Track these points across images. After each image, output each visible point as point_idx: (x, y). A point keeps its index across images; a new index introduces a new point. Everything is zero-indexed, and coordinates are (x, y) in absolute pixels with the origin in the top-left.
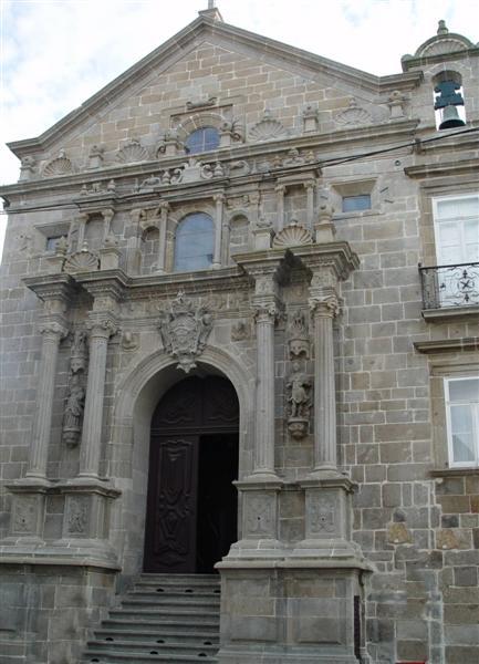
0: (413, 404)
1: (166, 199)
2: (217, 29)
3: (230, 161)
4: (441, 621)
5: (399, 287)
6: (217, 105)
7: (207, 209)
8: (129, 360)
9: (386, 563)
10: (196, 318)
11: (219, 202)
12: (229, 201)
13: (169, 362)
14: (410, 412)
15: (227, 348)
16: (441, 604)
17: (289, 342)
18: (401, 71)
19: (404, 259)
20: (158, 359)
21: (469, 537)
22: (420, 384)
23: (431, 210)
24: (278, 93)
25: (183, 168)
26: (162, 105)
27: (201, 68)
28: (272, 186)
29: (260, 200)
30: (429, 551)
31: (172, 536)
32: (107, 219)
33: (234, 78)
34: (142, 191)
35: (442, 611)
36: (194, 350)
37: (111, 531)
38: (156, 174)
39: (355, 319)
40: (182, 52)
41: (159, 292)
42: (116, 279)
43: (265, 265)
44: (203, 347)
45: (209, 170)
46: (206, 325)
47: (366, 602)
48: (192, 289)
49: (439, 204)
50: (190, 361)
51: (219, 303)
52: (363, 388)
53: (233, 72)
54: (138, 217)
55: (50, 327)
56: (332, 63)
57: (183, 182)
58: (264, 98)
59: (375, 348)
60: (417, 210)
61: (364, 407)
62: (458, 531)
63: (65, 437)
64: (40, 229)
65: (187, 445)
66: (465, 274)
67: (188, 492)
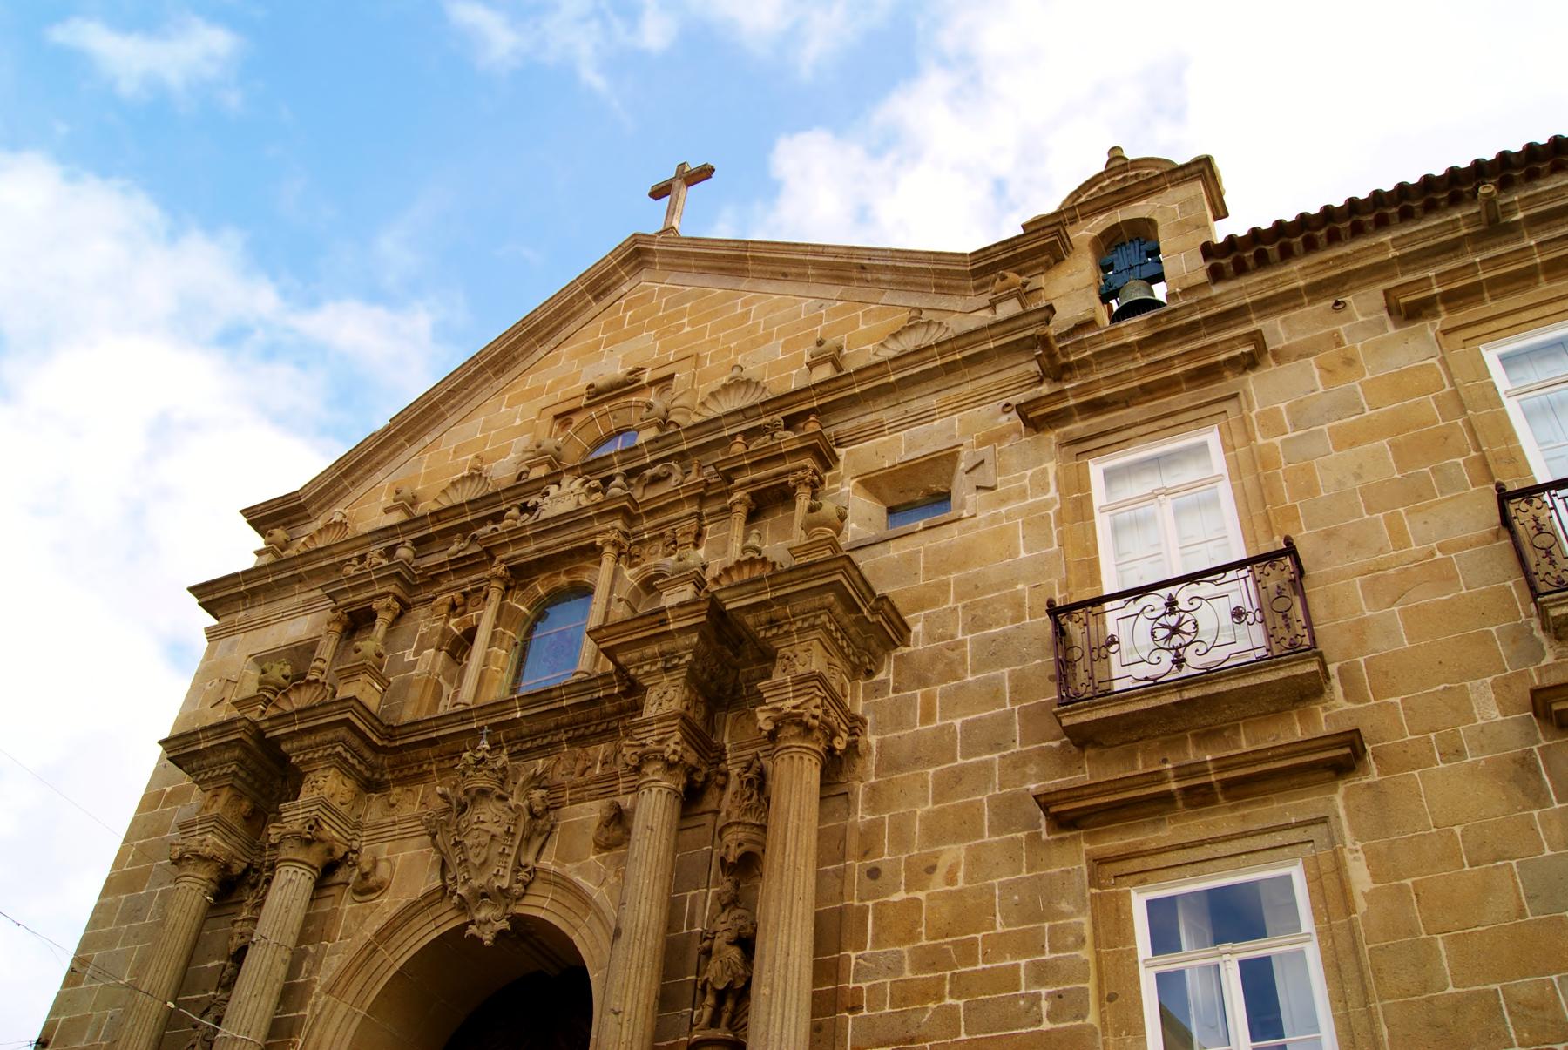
0: (1041, 973)
5: (1006, 671)
6: (645, 382)
10: (512, 802)
11: (608, 549)
13: (449, 921)
14: (1037, 997)
19: (1021, 605)
22: (1062, 915)
24: (768, 337)
26: (544, 400)
27: (626, 326)
33: (687, 329)
36: (505, 884)
39: (890, 763)
40: (596, 307)
42: (347, 722)
43: (666, 646)
44: (530, 878)
45: (596, 490)
48: (522, 738)
49: (1111, 476)
50: (499, 913)
51: (580, 766)
52: (902, 942)
53: (686, 320)
54: (445, 608)
58: (738, 352)
59: (936, 832)
60: (1053, 493)
61: (906, 995)
66: (1171, 604)
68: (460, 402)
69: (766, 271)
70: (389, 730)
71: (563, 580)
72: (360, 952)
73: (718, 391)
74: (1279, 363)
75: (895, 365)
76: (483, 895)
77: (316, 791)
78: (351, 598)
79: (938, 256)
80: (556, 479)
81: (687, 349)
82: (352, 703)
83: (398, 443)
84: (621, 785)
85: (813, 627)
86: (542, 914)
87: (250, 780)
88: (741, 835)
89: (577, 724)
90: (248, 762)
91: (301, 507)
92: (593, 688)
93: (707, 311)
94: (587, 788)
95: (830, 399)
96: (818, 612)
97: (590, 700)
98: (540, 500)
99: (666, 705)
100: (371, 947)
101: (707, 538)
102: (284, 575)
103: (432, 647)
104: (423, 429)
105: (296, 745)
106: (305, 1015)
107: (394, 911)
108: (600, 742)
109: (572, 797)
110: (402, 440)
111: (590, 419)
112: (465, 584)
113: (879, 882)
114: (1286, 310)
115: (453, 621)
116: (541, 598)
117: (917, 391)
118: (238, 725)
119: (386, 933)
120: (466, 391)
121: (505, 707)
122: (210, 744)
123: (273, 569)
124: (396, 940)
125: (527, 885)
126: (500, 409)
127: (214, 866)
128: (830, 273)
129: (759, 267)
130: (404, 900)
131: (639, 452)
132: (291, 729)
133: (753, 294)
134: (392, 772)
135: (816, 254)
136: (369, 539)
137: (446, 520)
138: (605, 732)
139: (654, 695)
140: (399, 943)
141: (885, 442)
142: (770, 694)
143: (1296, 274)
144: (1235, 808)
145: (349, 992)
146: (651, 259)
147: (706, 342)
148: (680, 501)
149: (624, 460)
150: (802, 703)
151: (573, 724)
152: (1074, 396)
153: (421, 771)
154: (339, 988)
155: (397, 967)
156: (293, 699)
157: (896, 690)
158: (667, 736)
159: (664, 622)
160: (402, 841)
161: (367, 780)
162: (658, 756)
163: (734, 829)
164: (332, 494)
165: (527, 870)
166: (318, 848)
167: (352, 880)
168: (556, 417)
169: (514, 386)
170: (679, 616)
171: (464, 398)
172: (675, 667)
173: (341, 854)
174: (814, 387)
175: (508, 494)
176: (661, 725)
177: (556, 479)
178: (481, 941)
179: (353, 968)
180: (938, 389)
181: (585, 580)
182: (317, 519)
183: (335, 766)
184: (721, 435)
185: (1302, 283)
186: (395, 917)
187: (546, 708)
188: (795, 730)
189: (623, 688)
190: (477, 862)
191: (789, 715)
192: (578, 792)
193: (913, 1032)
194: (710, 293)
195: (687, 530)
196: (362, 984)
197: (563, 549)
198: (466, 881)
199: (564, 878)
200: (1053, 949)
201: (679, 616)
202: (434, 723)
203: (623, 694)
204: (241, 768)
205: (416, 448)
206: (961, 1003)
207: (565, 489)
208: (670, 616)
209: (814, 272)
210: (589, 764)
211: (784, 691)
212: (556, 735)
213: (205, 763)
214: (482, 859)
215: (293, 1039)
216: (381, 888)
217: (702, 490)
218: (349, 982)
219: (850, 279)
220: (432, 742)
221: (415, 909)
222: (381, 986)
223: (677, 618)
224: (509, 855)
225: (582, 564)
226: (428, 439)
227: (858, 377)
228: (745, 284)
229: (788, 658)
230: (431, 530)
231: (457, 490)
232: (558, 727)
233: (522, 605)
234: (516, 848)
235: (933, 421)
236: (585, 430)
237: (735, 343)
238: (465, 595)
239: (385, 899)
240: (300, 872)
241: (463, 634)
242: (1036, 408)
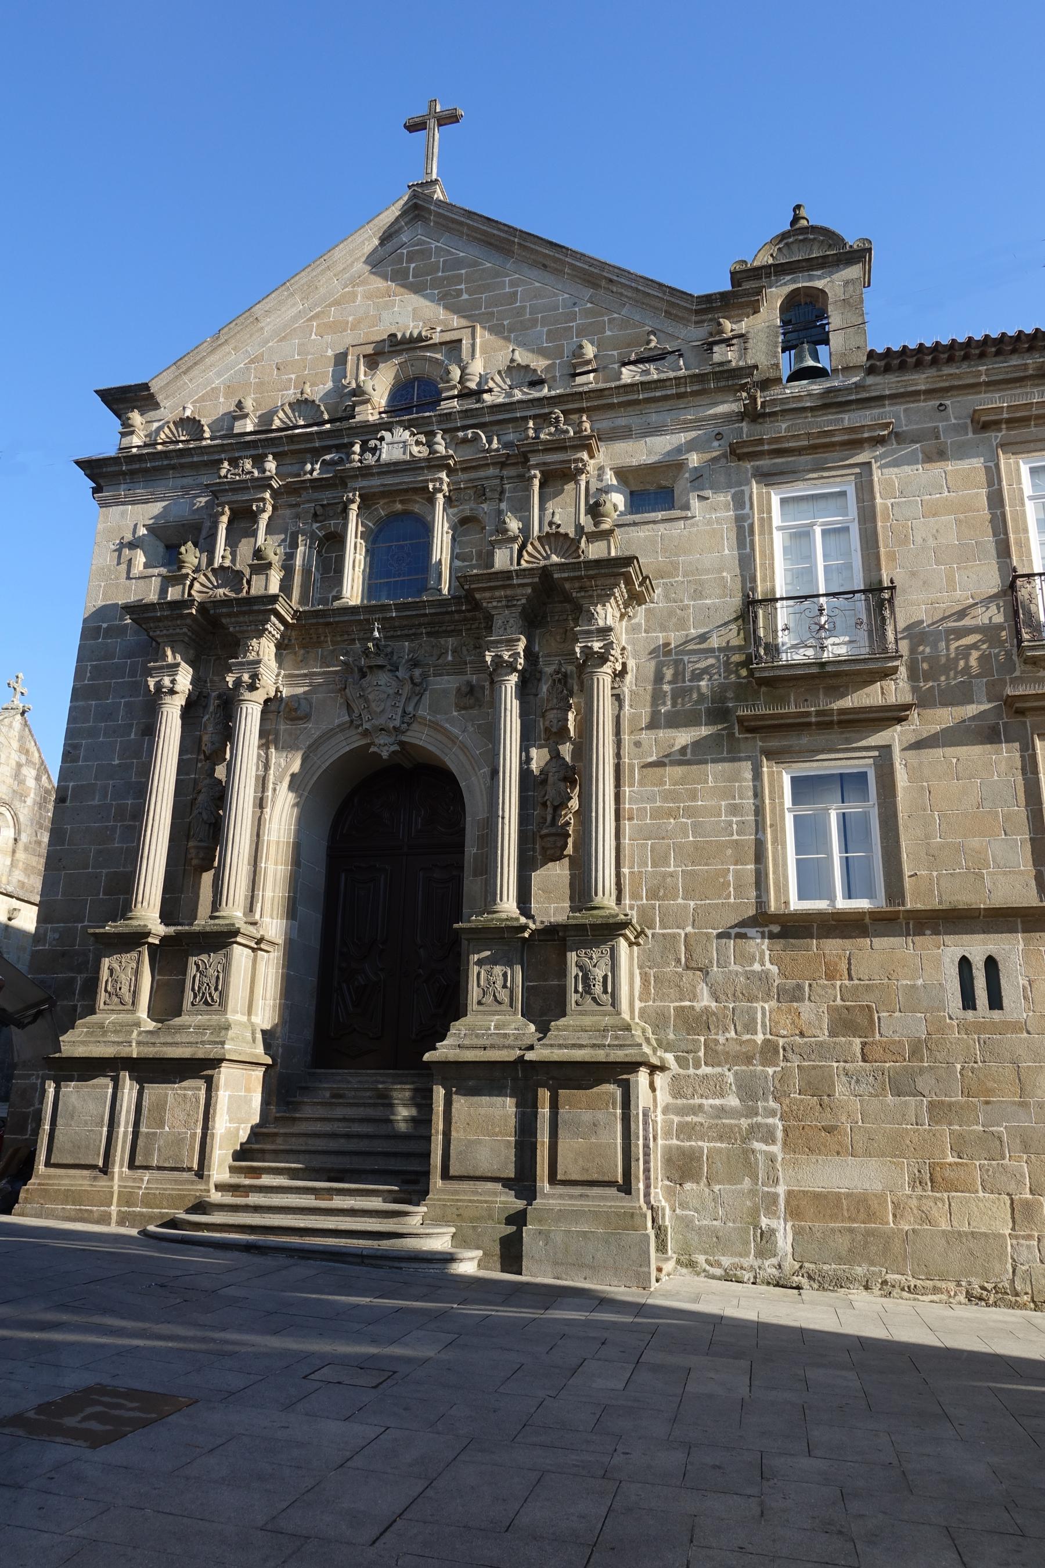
2: (439, 215)
3: (458, 429)
4: (776, 1149)
9: (690, 1056)
10: (399, 674)
16: (775, 1121)
17: (543, 716)
18: (728, 287)
20: (340, 737)
21: (820, 1019)
23: (769, 512)
24: (534, 322)
25: (382, 439)
27: (411, 279)
28: (521, 470)
29: (502, 492)
30: (759, 1038)
35: (779, 1134)
36: (397, 723)
38: (338, 448)
43: (509, 592)
44: (409, 719)
47: (660, 1118)
48: (394, 629)
50: (391, 740)
53: (463, 286)
62: (806, 1009)
71: (399, 507)
74: (899, 444)
80: (388, 426)
98: (378, 443)
105: (233, 620)
113: (641, 750)
114: (909, 402)
115: (315, 525)
125: (409, 724)
137: (299, 443)
138: (452, 631)
143: (920, 380)
144: (842, 733)
146: (427, 216)
147: (483, 314)
148: (488, 465)
152: (769, 444)
155: (324, 767)
157: (645, 632)
172: (514, 605)
175: (348, 432)
177: (388, 426)
178: (381, 756)
185: (923, 388)
186: (320, 737)
189: (469, 607)
190: (378, 710)
193: (664, 834)
200: (741, 798)
203: (468, 611)
206: (689, 821)
213: (161, 624)
232: (420, 625)
238: (322, 505)
242: (742, 447)
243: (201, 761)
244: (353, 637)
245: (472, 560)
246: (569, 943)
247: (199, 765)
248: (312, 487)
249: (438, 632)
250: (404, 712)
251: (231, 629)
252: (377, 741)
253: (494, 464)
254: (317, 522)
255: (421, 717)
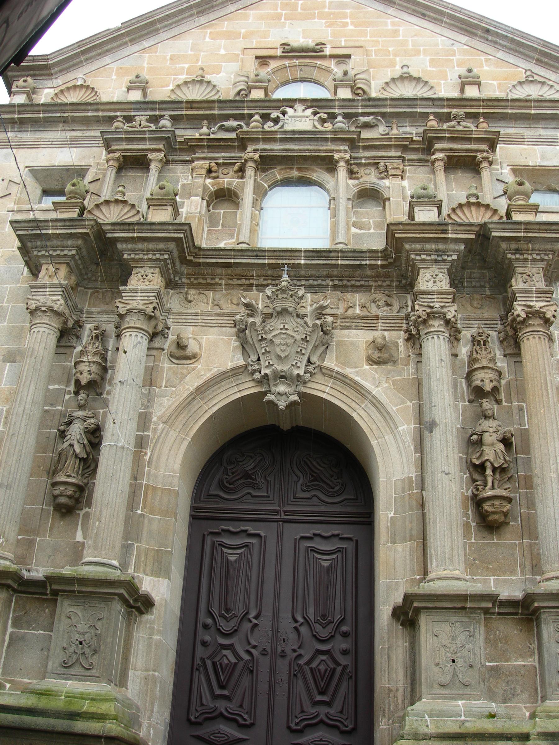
1: (256, 151)
7: (318, 175)
8: (183, 377)
11: (342, 164)
12: (355, 169)
15: (357, 373)
24: (418, 53)
25: (284, 113)
27: (299, 10)
31: (226, 692)
32: (153, 167)
34: (212, 136)
37: (131, 673)
38: (236, 117)
41: (240, 277)
43: (441, 246)
46: (325, 333)
51: (342, 306)
53: (348, 20)
54: (204, 172)
55: (49, 304)
56: (498, 24)
57: (288, 128)
58: (396, 55)
63: (56, 492)
64: (35, 172)
65: (258, 535)
67: (256, 617)
68: (171, 24)
69: (409, 8)
70: (197, 250)
71: (295, 173)
72: (185, 399)
73: (397, 79)
75: (536, 104)
76: (283, 377)
77: (147, 283)
78: (124, 146)
79: (546, 44)
81: (355, 41)
82: (186, 227)
83: (124, 40)
84: (380, 324)
85: (542, 260)
86: (324, 396)
87: (79, 262)
88: (491, 375)
89: (343, 277)
90: (84, 250)
91: (47, 67)
92: (362, 257)
93: (364, 20)
94: (354, 321)
95: (492, 111)
96: (548, 252)
97: (359, 265)
98: (281, 115)
99: (439, 284)
100: (192, 396)
101: (408, 175)
102: (54, 115)
103: (197, 196)
104: (142, 36)
105: (130, 246)
106: (148, 436)
107: (209, 375)
108: (356, 292)
109: (341, 324)
110: (127, 39)
111: (284, 66)
112: (219, 157)
115: (208, 181)
116: (277, 182)
117: (542, 124)
118: (87, 223)
119: (203, 389)
120: (177, 19)
121: (293, 254)
122: (58, 232)
123: (45, 108)
124: (209, 394)
125: (312, 374)
126: (204, 39)
127: (62, 319)
128: (461, 26)
129: (405, 4)
130: (216, 370)
131: (355, 104)
132: (131, 235)
133: (397, 20)
134: (189, 279)
135: (455, 11)
136: (132, 106)
138: (361, 286)
139: (428, 275)
140: (211, 397)
141: (525, 149)
142: (521, 295)
145: (177, 423)
149: (343, 106)
150: (544, 306)
151: (341, 277)
153: (213, 282)
154: (171, 421)
155: (210, 413)
156: (104, 210)
158: (447, 304)
159: (445, 231)
160: (204, 328)
161: (170, 280)
162: (442, 316)
163: (486, 371)
164: (71, 63)
165: (314, 366)
166: (153, 323)
167: (166, 346)
168: (257, 57)
169: (213, 25)
170: (457, 230)
171: (175, 22)
172: (444, 261)
173: (160, 329)
174: (483, 100)
176: (439, 296)
177: (290, 104)
179: (180, 409)
180: (556, 127)
181: (314, 178)
182: (56, 78)
183: (159, 268)
184: (415, 110)
186: (211, 380)
187: (325, 262)
188: (538, 321)
189: (384, 263)
191: (537, 312)
192: (348, 322)
194: (364, 8)
195: (395, 166)
196: (185, 420)
197: (304, 154)
198: (270, 365)
199: (345, 377)
201: (457, 230)
202: (233, 253)
203: (382, 266)
204: (78, 254)
205: (136, 47)
207: (299, 113)
208: (450, 228)
209: (448, 21)
210: (351, 305)
211: (530, 295)
212: (325, 280)
214: (287, 354)
215: (144, 450)
216: (195, 358)
217: (408, 143)
218: (177, 417)
219: (476, 35)
220: (228, 265)
221: (224, 376)
222: (200, 423)
223: (455, 231)
224: (303, 354)
225: (312, 167)
226: (146, 44)
227: (512, 104)
228: (391, 11)
229: (529, 276)
230: (184, 113)
231: (188, 88)
232: (328, 276)
233: (266, 183)
234: (309, 351)
235: (556, 145)
236: (279, 72)
237: (393, 48)
238: (216, 163)
239: (199, 366)
240: (145, 337)
241: (215, 191)
243: (69, 392)
244: (252, 281)
245: (369, 229)
246: (544, 616)
247: (67, 397)
248: (209, 146)
249: (345, 286)
250: (309, 361)
251: (125, 256)
252: (274, 389)
253: (397, 146)
254: (210, 178)
255: (327, 369)
